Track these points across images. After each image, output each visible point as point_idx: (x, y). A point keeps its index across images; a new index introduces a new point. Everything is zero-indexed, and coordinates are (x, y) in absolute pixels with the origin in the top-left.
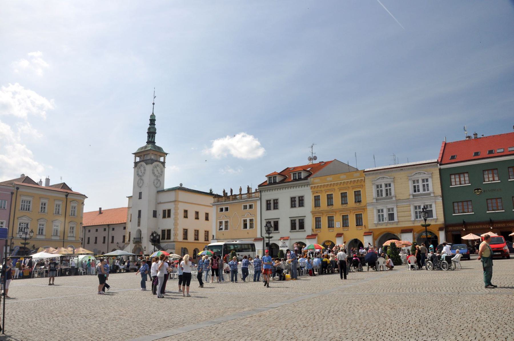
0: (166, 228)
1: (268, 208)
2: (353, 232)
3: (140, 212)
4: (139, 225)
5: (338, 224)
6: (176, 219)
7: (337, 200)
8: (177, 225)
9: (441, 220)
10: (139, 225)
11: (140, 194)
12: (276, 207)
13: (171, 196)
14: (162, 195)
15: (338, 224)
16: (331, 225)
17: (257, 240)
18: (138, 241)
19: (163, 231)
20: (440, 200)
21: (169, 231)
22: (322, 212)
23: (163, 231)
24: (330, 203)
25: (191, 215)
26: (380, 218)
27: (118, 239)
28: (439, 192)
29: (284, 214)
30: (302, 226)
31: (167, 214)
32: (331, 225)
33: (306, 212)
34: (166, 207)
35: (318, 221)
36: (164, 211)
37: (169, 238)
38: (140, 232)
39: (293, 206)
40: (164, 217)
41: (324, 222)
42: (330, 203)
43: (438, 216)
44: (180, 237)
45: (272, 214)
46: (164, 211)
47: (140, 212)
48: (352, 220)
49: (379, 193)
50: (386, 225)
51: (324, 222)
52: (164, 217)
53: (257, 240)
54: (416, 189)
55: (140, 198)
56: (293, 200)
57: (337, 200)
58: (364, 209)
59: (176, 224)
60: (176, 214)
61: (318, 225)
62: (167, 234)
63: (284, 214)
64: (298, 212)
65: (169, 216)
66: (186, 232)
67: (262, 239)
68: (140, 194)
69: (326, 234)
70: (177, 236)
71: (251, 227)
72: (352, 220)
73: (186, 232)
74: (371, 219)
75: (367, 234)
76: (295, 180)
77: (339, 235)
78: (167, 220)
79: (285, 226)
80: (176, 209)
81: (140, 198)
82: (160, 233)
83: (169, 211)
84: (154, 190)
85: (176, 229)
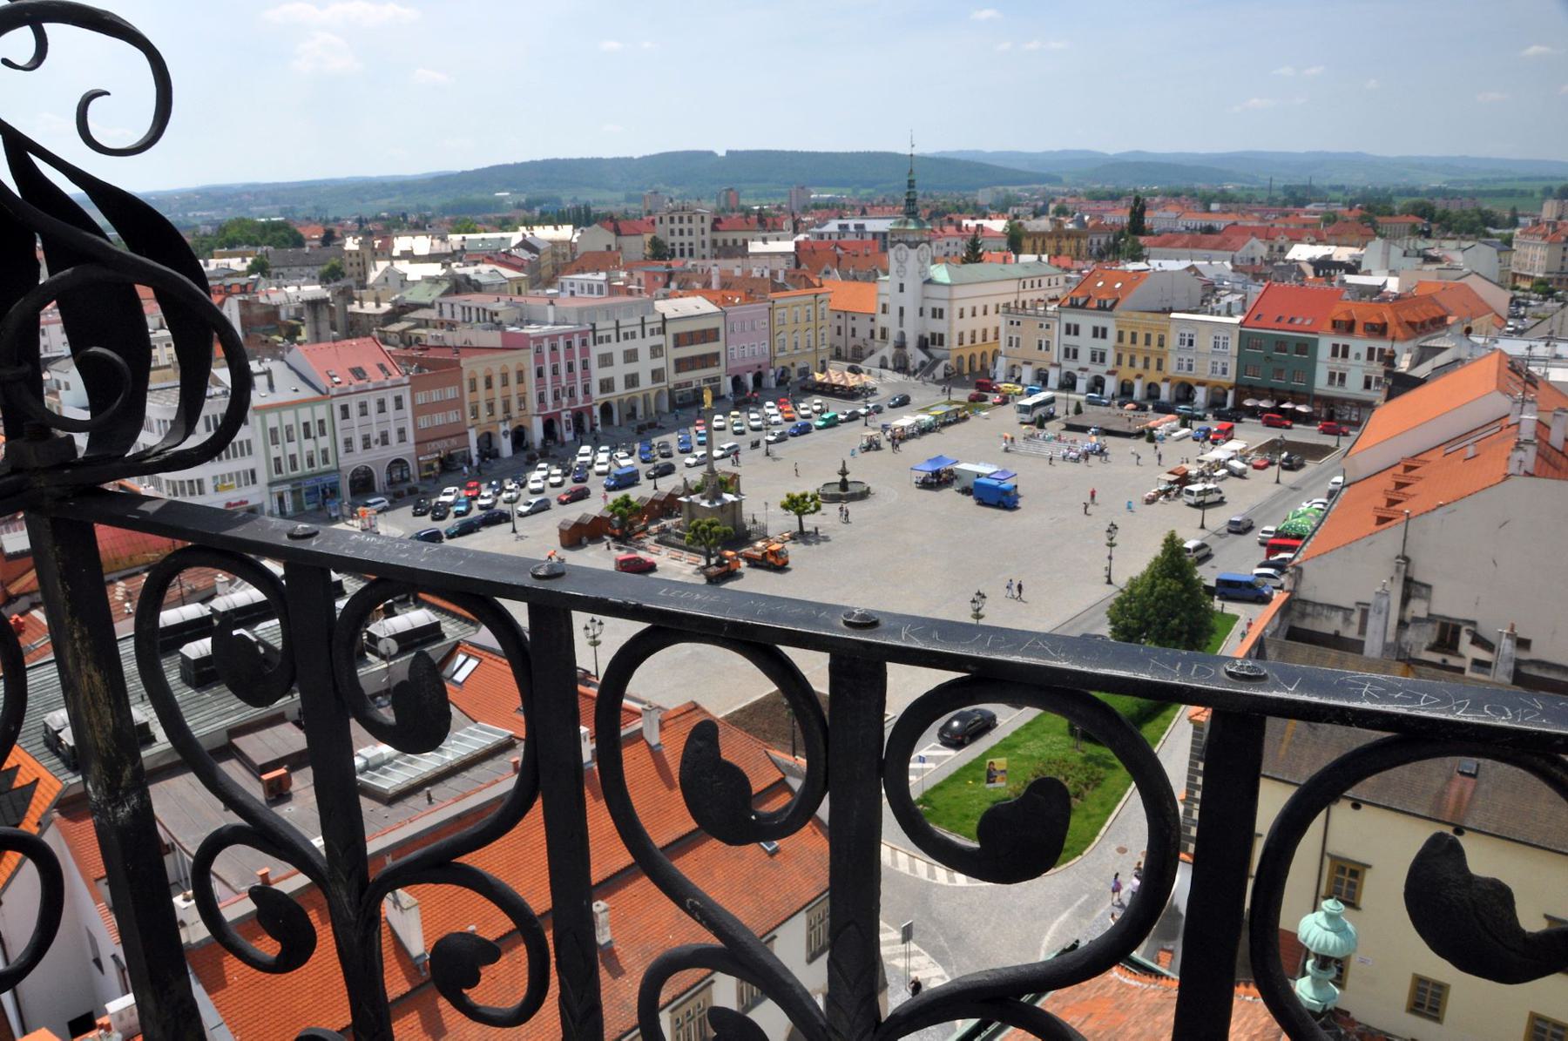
0: (938, 330)
1: (1068, 332)
2: (1153, 376)
3: (901, 310)
4: (901, 324)
5: (1139, 364)
6: (950, 322)
7: (1141, 340)
8: (954, 328)
9: (1233, 380)
10: (901, 324)
11: (902, 286)
12: (1076, 333)
13: (944, 293)
14: (929, 287)
15: (1139, 364)
16: (1132, 365)
17: (1053, 365)
18: (901, 345)
19: (933, 335)
20: (1235, 361)
21: (941, 336)
22: (1124, 349)
23: (933, 335)
24: (1134, 341)
25: (968, 313)
26: (1180, 367)
27: (863, 333)
28: (1235, 352)
29: (1085, 343)
30: (1102, 360)
31: (938, 314)
32: (1132, 365)
33: (1108, 344)
34: (938, 305)
35: (1119, 357)
36: (934, 310)
37: (941, 343)
38: (902, 334)
39: (1095, 335)
40: (934, 316)
41: (1126, 360)
42: (1134, 341)
43: (1231, 376)
44: (955, 345)
45: (1071, 340)
46: (934, 310)
47: (901, 310)
48: (1153, 363)
49: (1182, 342)
50: (1184, 375)
51: (1126, 360)
52: (934, 316)
53: (1053, 365)
54: (1216, 345)
55: (902, 290)
56: (1095, 330)
57: (1141, 340)
58: (1165, 354)
59: (950, 328)
60: (951, 316)
61: (1119, 362)
62: (938, 339)
63: (1085, 343)
64: (1099, 344)
65: (941, 317)
66: (961, 335)
67: (1059, 365)
68: (902, 286)
69: (1126, 373)
70: (952, 342)
71: (1047, 349)
72: (1153, 363)
73: (961, 335)
74: (1171, 367)
75: (1166, 380)
76: (1099, 308)
77: (1139, 376)
78: (937, 321)
79: (1084, 357)
80: (951, 309)
81: (902, 290)
82: (928, 336)
83: (941, 311)
84: (920, 281)
85: (950, 334)
